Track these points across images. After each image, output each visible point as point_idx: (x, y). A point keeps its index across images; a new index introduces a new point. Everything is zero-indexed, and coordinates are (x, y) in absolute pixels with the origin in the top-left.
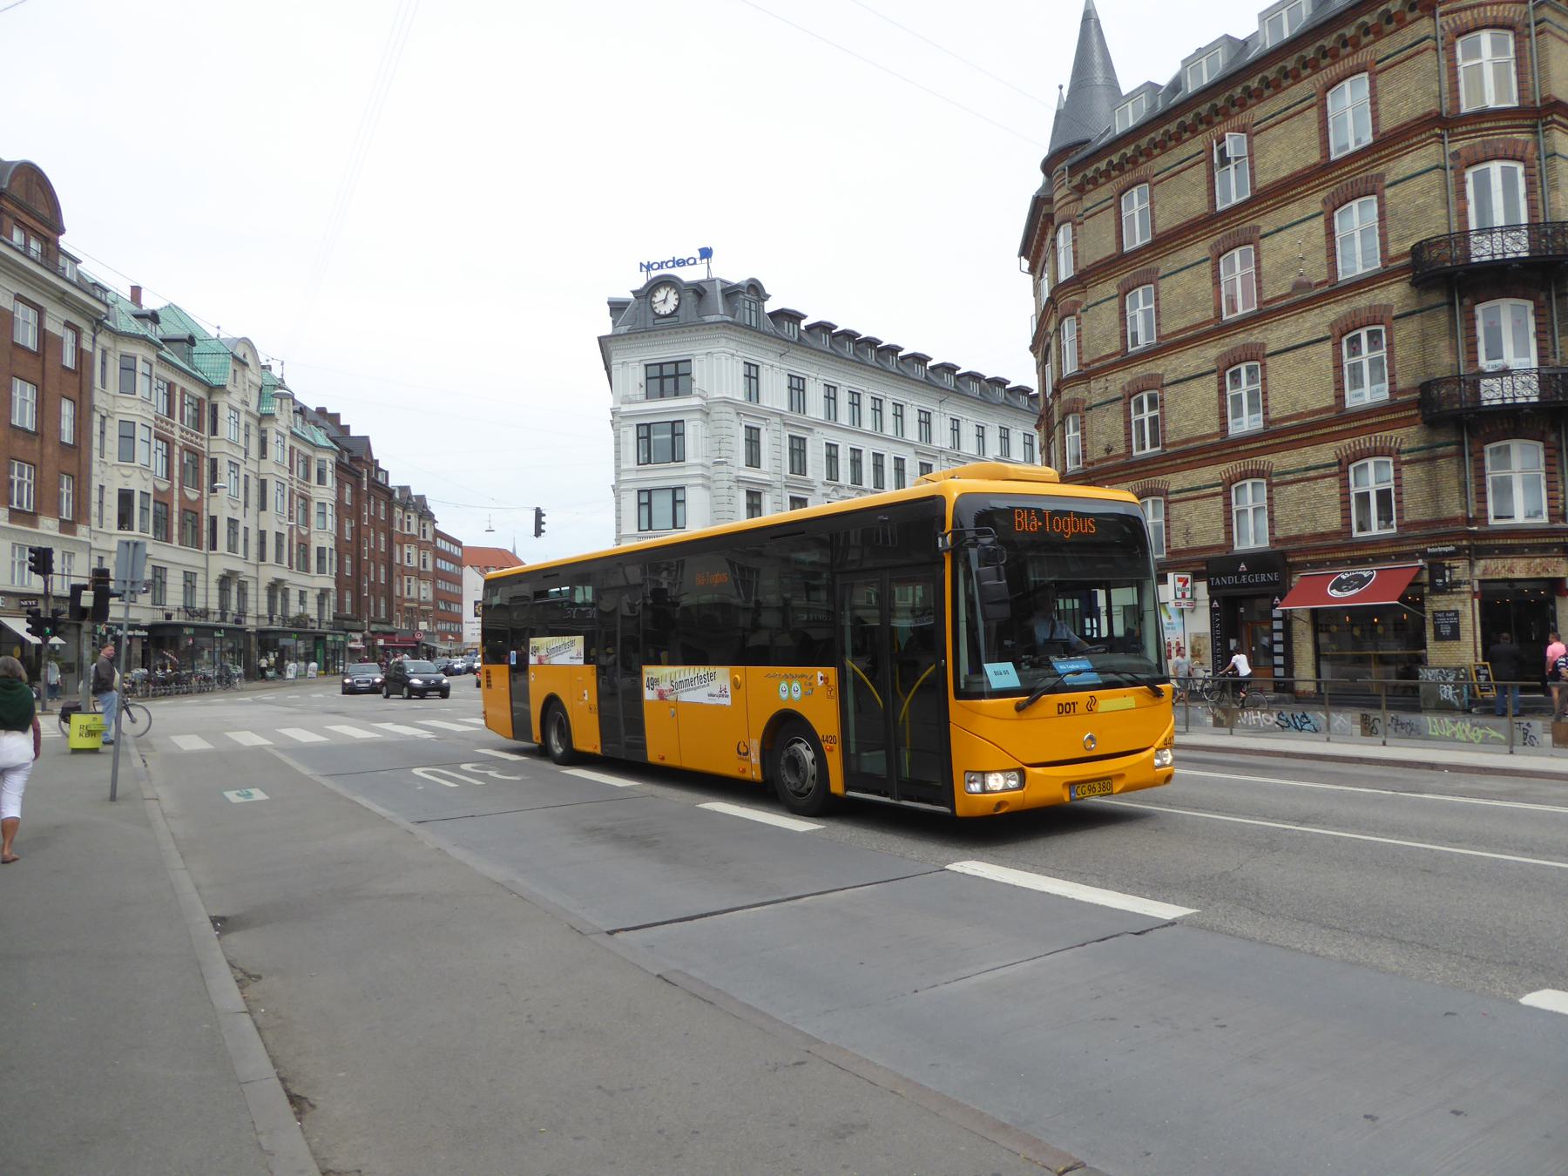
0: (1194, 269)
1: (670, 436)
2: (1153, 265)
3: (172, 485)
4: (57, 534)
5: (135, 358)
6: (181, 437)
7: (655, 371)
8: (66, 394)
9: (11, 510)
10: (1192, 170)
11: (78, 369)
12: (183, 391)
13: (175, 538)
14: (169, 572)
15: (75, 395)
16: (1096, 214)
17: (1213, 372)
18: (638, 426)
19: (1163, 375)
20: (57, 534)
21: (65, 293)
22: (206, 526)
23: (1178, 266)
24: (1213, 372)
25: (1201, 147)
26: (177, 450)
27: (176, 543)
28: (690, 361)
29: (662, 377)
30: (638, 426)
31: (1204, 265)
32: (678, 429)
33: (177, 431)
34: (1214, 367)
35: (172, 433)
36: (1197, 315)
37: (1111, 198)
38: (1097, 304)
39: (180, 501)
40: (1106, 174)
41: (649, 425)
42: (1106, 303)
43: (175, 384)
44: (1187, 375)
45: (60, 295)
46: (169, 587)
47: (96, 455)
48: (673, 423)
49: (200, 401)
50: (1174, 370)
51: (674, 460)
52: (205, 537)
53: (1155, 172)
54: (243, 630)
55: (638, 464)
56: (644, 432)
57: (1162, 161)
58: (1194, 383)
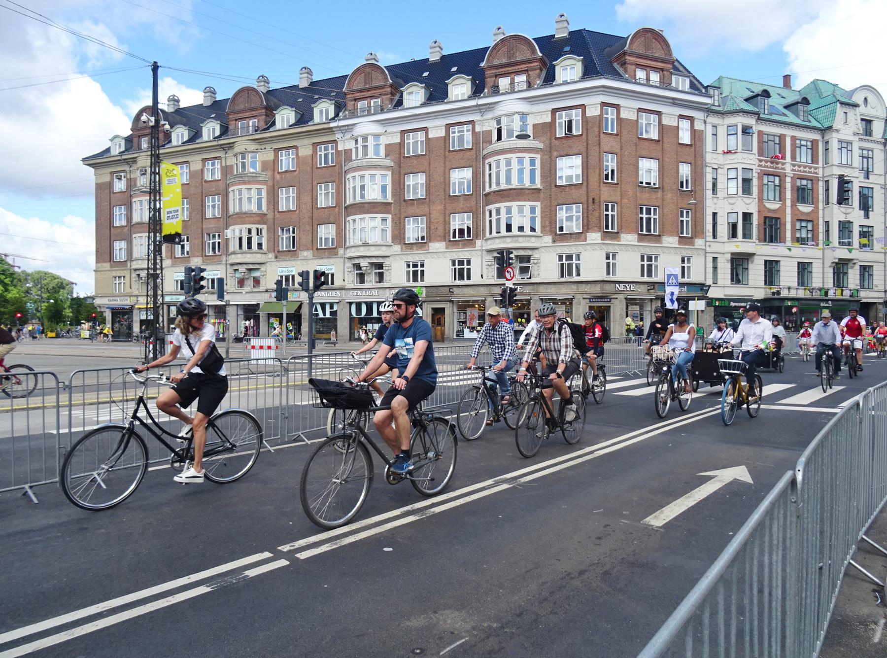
3: (784, 204)
4: (677, 246)
5: (737, 126)
6: (793, 170)
8: (682, 160)
9: (639, 234)
11: (693, 143)
12: (794, 139)
13: (821, 242)
14: (782, 263)
15: (691, 159)
20: (677, 246)
21: (673, 99)
22: (821, 229)
26: (788, 180)
27: (789, 243)
33: (788, 169)
35: (784, 169)
39: (793, 215)
43: (785, 135)
45: (671, 101)
46: (814, 275)
47: (709, 193)
49: (814, 143)
52: (821, 236)
54: (858, 301)
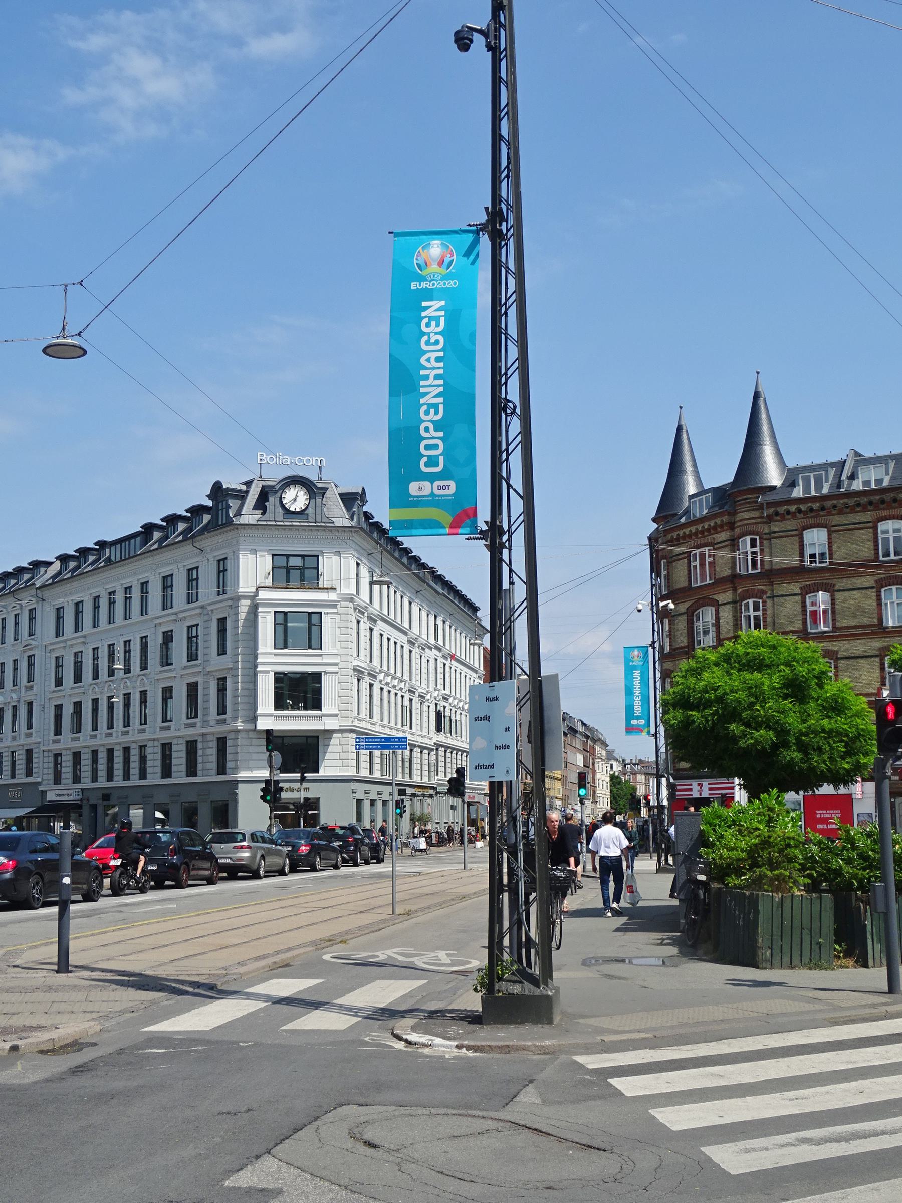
0: (864, 592)
1: (306, 625)
2: (834, 581)
7: (282, 562)
10: (863, 531)
16: (782, 537)
17: (877, 656)
18: (275, 612)
19: (837, 652)
23: (851, 587)
24: (877, 656)
25: (870, 519)
28: (317, 557)
29: (288, 569)
30: (275, 612)
31: (871, 591)
32: (315, 619)
34: (878, 653)
36: (865, 620)
37: (796, 530)
38: (782, 596)
40: (793, 515)
41: (285, 613)
42: (791, 597)
44: (857, 655)
48: (310, 614)
50: (847, 650)
51: (310, 647)
53: (833, 524)
55: (275, 648)
56: (280, 618)
57: (837, 519)
58: (862, 661)
